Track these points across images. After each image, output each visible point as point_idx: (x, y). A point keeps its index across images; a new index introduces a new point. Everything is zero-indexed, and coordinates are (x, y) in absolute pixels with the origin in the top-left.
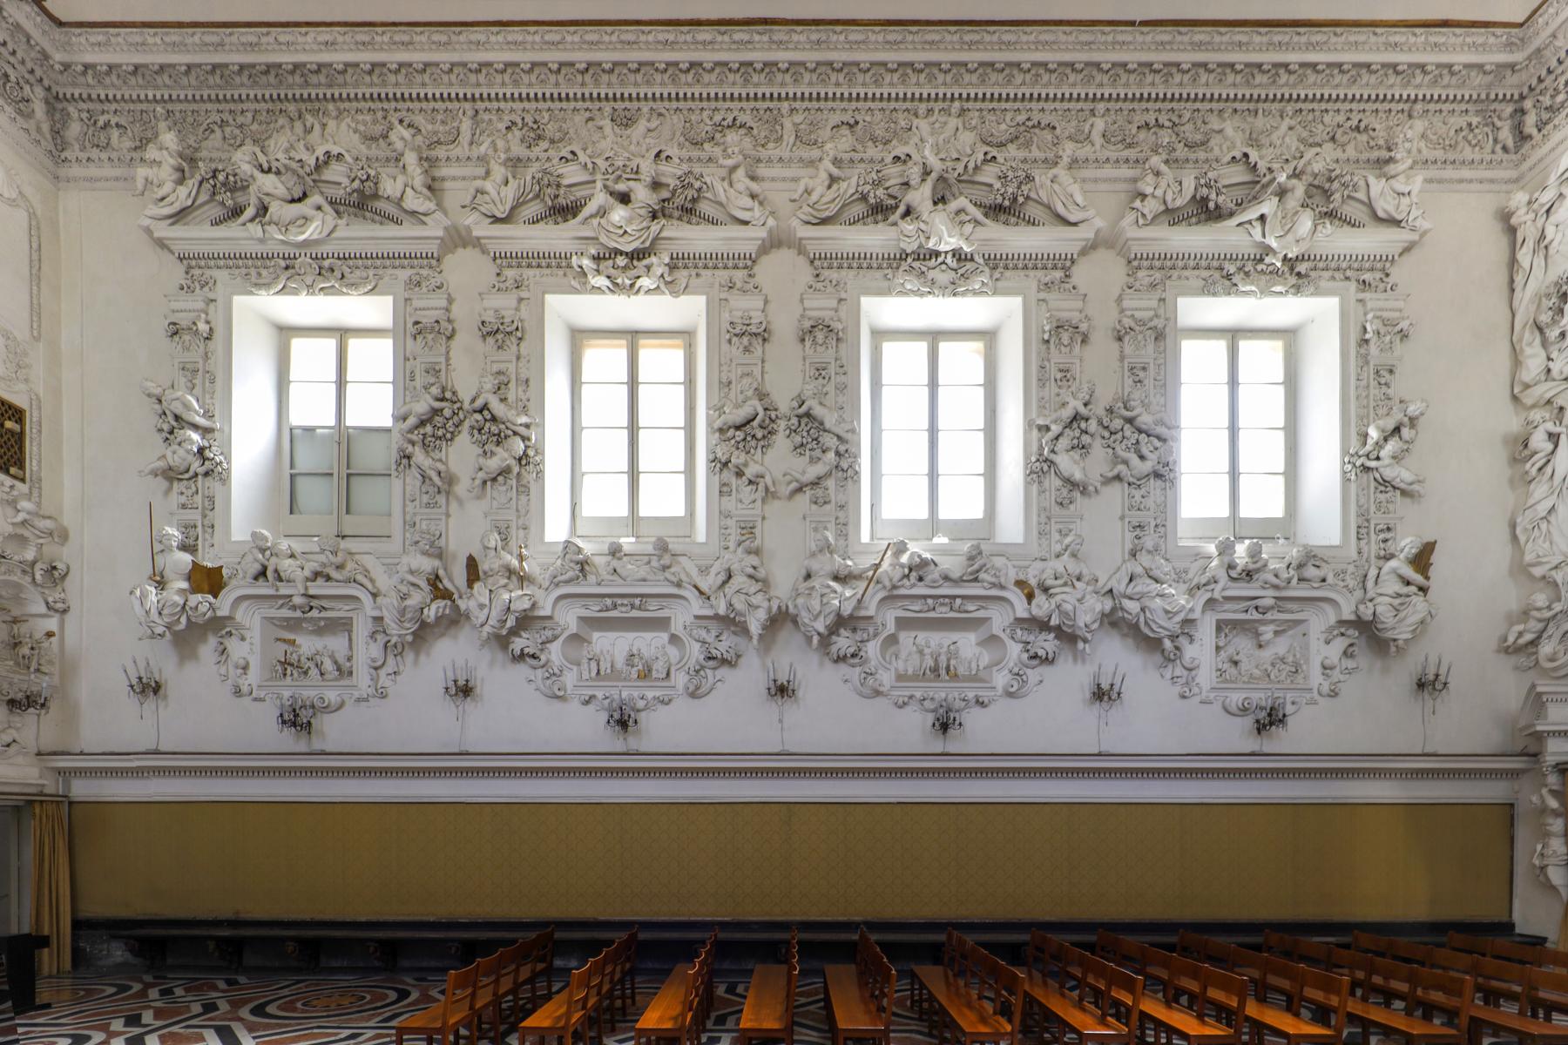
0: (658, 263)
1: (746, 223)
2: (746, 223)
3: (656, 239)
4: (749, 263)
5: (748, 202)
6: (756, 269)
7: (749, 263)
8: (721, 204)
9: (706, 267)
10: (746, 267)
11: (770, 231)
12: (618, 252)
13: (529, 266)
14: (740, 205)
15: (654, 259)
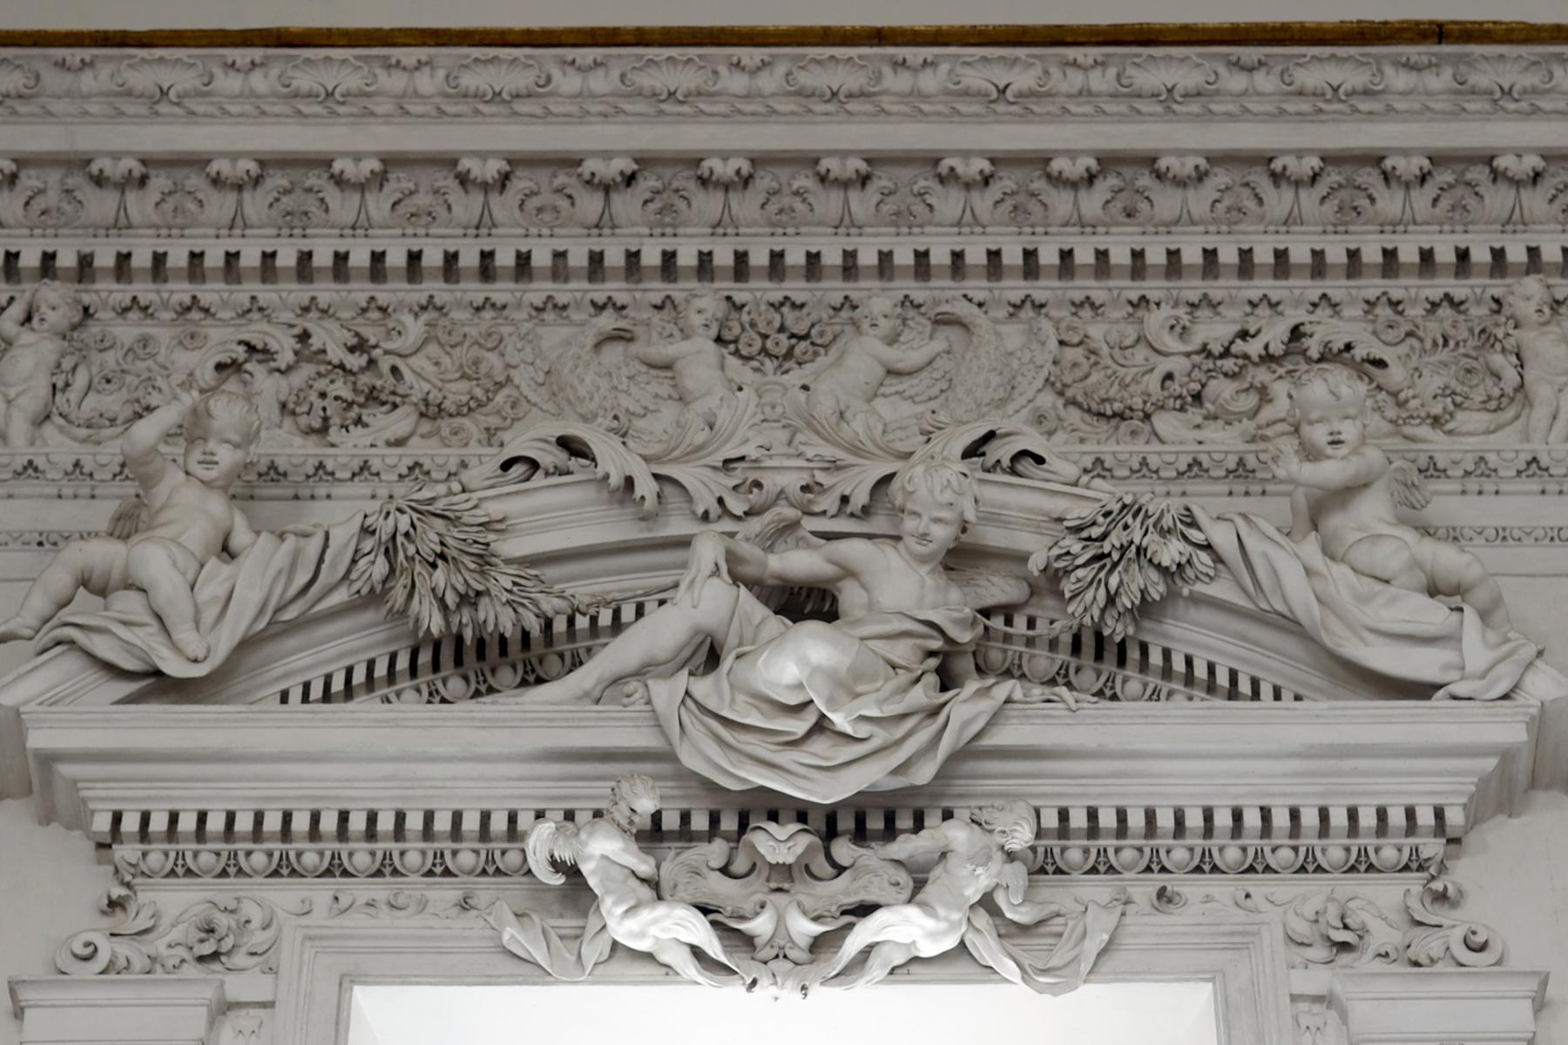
0: (969, 855)
1: (1421, 690)
2: (1421, 690)
3: (967, 752)
4: (1432, 847)
5: (1434, 615)
6: (1462, 873)
7: (1429, 851)
8: (1289, 624)
9: (1205, 866)
10: (1414, 864)
11: (1540, 723)
12: (774, 808)
13: (284, 869)
14: (1383, 622)
15: (957, 834)
